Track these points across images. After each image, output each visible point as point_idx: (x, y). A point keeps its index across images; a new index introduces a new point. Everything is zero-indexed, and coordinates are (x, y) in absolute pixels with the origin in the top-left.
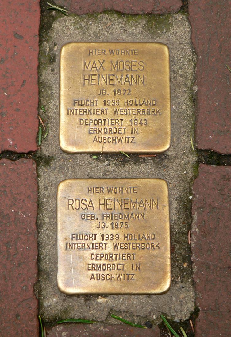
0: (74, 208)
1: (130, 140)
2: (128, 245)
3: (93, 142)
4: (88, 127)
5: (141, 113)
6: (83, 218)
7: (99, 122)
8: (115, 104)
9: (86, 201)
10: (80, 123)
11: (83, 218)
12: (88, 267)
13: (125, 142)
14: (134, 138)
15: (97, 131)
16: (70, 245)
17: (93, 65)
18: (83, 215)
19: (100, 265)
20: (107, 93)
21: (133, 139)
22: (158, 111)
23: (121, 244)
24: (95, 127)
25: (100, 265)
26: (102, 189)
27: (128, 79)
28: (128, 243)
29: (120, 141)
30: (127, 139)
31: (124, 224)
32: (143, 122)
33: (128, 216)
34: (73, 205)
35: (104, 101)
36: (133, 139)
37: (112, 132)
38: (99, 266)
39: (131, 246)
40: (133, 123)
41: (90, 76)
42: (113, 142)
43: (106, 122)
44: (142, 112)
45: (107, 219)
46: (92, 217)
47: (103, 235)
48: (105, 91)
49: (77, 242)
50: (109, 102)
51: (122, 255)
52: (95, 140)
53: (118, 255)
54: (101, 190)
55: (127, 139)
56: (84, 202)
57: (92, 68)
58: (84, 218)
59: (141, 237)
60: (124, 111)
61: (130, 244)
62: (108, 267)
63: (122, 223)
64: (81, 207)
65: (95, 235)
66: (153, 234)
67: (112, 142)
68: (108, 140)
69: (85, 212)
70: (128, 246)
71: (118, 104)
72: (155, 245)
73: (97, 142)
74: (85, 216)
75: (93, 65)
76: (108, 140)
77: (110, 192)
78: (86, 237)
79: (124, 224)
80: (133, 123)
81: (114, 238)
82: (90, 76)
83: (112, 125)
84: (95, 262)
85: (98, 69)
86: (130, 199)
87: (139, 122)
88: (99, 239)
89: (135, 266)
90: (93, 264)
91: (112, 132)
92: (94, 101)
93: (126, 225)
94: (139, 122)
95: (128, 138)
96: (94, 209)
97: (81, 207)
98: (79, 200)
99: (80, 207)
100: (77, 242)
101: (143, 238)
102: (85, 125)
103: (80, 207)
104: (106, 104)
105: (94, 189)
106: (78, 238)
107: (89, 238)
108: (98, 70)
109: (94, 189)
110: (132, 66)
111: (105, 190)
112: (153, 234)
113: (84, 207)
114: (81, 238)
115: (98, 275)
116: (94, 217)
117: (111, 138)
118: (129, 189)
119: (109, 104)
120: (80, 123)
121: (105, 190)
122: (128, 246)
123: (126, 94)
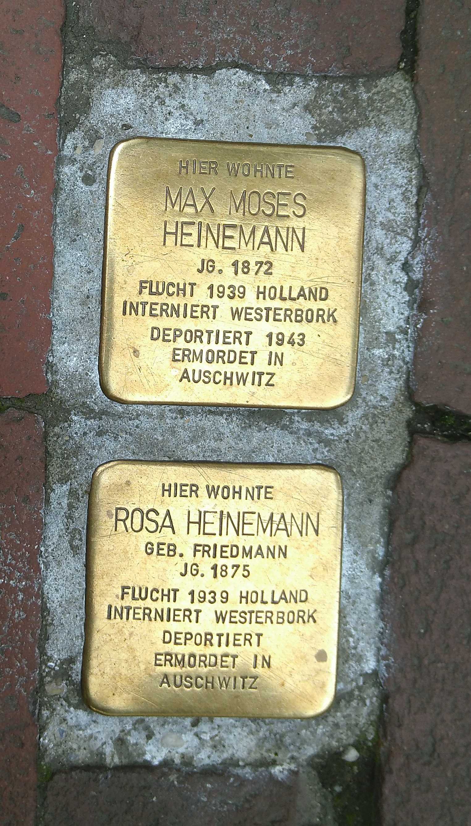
0: (130, 530)
1: (265, 379)
2: (248, 614)
3: (181, 381)
4: (172, 345)
5: (293, 317)
6: (149, 551)
7: (196, 335)
8: (234, 294)
9: (157, 514)
10: (152, 335)
11: (149, 551)
12: (156, 659)
13: (253, 384)
14: (273, 375)
15: (191, 356)
16: (116, 609)
17: (187, 199)
18: (149, 546)
19: (184, 656)
20: (217, 269)
21: (269, 381)
22: (330, 313)
23: (231, 612)
24: (187, 346)
25: (184, 656)
26: (194, 488)
27: (269, 237)
28: (247, 612)
29: (242, 380)
30: (257, 377)
31: (241, 568)
32: (297, 339)
33: (251, 551)
34: (128, 522)
35: (211, 288)
36: (269, 381)
37: (226, 358)
38: (180, 657)
39: (254, 615)
40: (274, 339)
41: (180, 225)
42: (225, 383)
43: (213, 336)
44: (297, 316)
45: (203, 556)
46: (169, 550)
47: (193, 591)
48: (197, 566)
49: (134, 604)
50: (221, 289)
51: (233, 636)
52: (185, 376)
53: (225, 636)
54: (192, 491)
55: (257, 377)
56: (152, 515)
57: (186, 204)
58: (152, 552)
59: (276, 599)
60: (256, 311)
61: (251, 612)
62: (200, 661)
63: (238, 566)
64: (146, 528)
65: (176, 591)
66: (303, 590)
67: (222, 382)
68: (214, 378)
69: (155, 539)
70: (248, 617)
71: (241, 295)
72: (306, 615)
73: (189, 381)
74: (155, 547)
75: (187, 199)
76: (214, 378)
77: (213, 496)
78: (154, 593)
79: (241, 568)
80: (274, 339)
81: (218, 598)
82: (180, 225)
83: (225, 343)
84: (171, 648)
85: (199, 209)
86: (257, 514)
87: (286, 339)
88: (183, 601)
89: (260, 659)
90: (167, 654)
91: (226, 358)
92: (187, 286)
93: (244, 570)
94: (286, 339)
95: (261, 374)
96: (174, 533)
97: (146, 528)
98: (142, 512)
99: (142, 526)
100: (134, 604)
101: (281, 598)
102: (164, 340)
103: (142, 526)
104: (196, 600)
105: (176, 489)
106: (137, 596)
107: (160, 597)
108: (199, 210)
109: (176, 489)
110: (279, 204)
111: (202, 492)
112: (303, 590)
113: (152, 527)
114: (143, 595)
115: (178, 678)
116: (174, 551)
117: (221, 374)
118: (256, 490)
119: (221, 295)
120: (152, 335)
121: (202, 492)
122: (248, 617)
123: (261, 273)
